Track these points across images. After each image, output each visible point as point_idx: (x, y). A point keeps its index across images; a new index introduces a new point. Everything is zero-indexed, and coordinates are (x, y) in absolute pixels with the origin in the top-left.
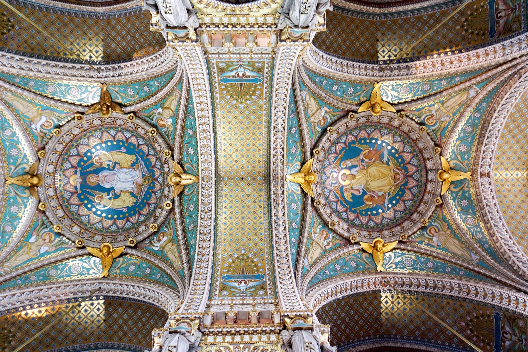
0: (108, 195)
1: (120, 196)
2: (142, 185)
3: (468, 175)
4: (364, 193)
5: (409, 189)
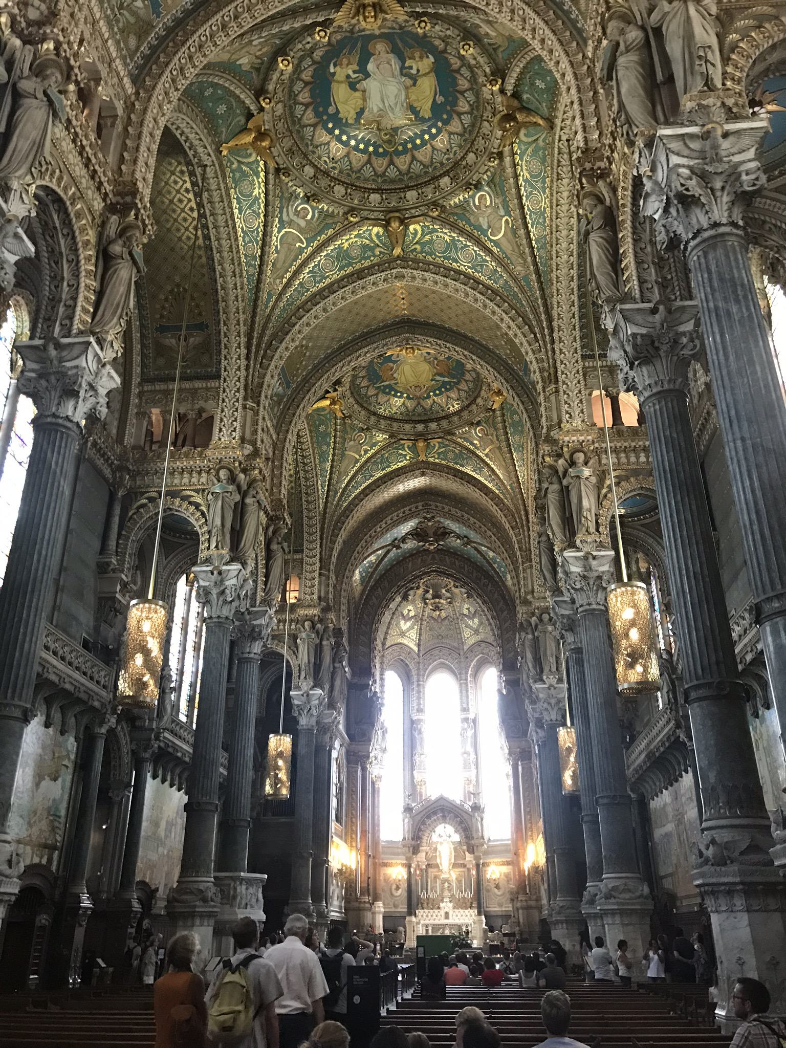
0: (355, 72)
1: (355, 90)
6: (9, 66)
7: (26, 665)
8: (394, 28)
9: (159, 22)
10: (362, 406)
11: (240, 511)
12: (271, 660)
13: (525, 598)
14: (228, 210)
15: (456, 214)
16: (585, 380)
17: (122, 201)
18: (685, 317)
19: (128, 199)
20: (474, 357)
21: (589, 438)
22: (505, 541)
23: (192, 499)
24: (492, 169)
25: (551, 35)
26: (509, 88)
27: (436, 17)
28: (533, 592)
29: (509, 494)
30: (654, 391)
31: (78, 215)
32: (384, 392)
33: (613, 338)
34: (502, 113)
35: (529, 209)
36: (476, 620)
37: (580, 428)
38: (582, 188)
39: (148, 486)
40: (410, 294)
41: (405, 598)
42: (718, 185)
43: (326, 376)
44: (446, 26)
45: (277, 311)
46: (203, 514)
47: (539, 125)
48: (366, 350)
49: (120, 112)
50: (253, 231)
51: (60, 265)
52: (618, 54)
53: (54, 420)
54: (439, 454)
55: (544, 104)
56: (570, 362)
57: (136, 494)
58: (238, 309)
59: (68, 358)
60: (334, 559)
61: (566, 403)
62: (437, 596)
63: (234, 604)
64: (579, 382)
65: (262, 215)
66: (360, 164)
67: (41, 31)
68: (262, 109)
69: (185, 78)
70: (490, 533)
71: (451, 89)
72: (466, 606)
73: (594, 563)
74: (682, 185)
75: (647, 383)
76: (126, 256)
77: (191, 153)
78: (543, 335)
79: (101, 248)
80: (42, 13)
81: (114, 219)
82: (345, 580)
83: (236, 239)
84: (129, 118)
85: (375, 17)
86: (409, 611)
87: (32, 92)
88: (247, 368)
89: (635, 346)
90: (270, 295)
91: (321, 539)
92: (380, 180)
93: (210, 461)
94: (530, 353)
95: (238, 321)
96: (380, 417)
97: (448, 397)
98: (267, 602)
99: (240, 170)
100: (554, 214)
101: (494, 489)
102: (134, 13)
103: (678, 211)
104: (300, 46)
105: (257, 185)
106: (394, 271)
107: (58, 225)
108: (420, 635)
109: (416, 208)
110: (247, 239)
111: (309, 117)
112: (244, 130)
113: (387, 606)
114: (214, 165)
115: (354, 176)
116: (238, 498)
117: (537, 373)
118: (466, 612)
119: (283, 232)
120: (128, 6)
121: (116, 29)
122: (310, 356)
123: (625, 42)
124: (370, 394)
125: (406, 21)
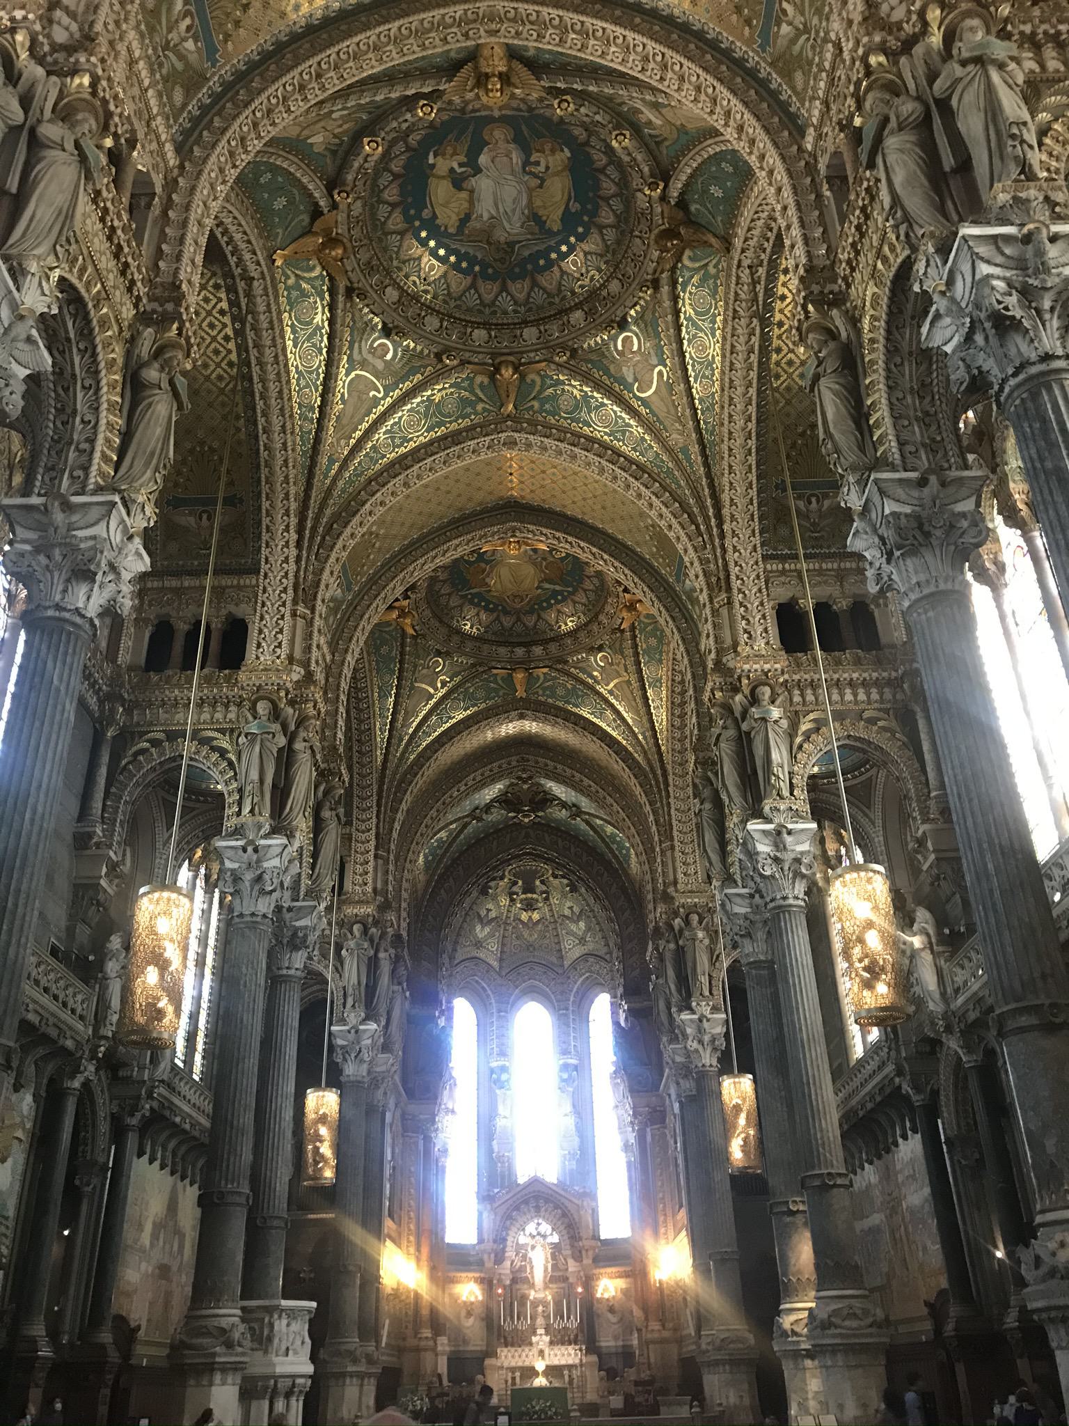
0: (461, 165)
2: (489, 243)
3: (521, 693)
4: (487, 562)
5: (498, 618)
6: (26, 102)
7: (11, 981)
8: (520, 110)
9: (214, 74)
10: (441, 621)
11: (286, 759)
12: (314, 979)
13: (665, 892)
14: (279, 341)
15: (591, 361)
16: (767, 588)
17: (160, 309)
18: (964, 491)
19: (170, 307)
20: (606, 557)
21: (778, 666)
22: (633, 810)
23: (215, 743)
24: (642, 302)
25: (753, 122)
26: (674, 193)
27: (582, 96)
28: (675, 883)
29: (642, 746)
30: (926, 591)
31: (104, 323)
32: (471, 603)
33: (861, 520)
34: (663, 227)
35: (691, 358)
36: (582, 924)
37: (764, 652)
38: (807, 318)
39: (151, 724)
40: (521, 468)
41: (484, 892)
42: (1047, 304)
43: (401, 576)
44: (595, 109)
45: (341, 484)
46: (231, 764)
47: (711, 246)
48: (456, 542)
49: (158, 190)
50: (311, 373)
51: (71, 395)
52: (886, 132)
53: (57, 614)
54: (545, 689)
55: (719, 219)
56: (747, 564)
57: (132, 733)
58: (287, 477)
59: (81, 524)
60: (395, 835)
61: (743, 617)
62: (529, 889)
63: (275, 895)
64: (760, 590)
65: (325, 350)
66: (462, 287)
67: (72, 60)
68: (334, 206)
69: (246, 152)
70: (609, 800)
71: (591, 194)
72: (569, 904)
73: (789, 840)
74: (999, 302)
75: (914, 581)
76: (165, 385)
77: (233, 261)
78: (709, 528)
79: (130, 372)
80: (71, 35)
81: (149, 332)
82: (408, 865)
83: (288, 382)
84: (170, 199)
85: (502, 90)
86: (488, 910)
87: (58, 140)
88: (298, 559)
89: (899, 530)
90: (331, 461)
91: (379, 805)
92: (487, 311)
93: (243, 688)
94: (691, 551)
95: (287, 494)
96: (466, 637)
97: (559, 611)
98: (313, 894)
99: (298, 287)
100: (728, 364)
101: (620, 738)
102: (181, 57)
103: (986, 339)
104: (395, 124)
105: (320, 309)
106: (503, 435)
107: (72, 335)
108: (503, 945)
109: (536, 350)
110: (303, 383)
111: (396, 221)
112: (308, 232)
113: (461, 902)
114: (264, 278)
115: (452, 304)
116: (282, 741)
117: (701, 578)
118: (567, 912)
119: (353, 375)
120: (175, 46)
121: (158, 76)
122: (380, 548)
123: (898, 117)
124: (452, 604)
125: (541, 100)
